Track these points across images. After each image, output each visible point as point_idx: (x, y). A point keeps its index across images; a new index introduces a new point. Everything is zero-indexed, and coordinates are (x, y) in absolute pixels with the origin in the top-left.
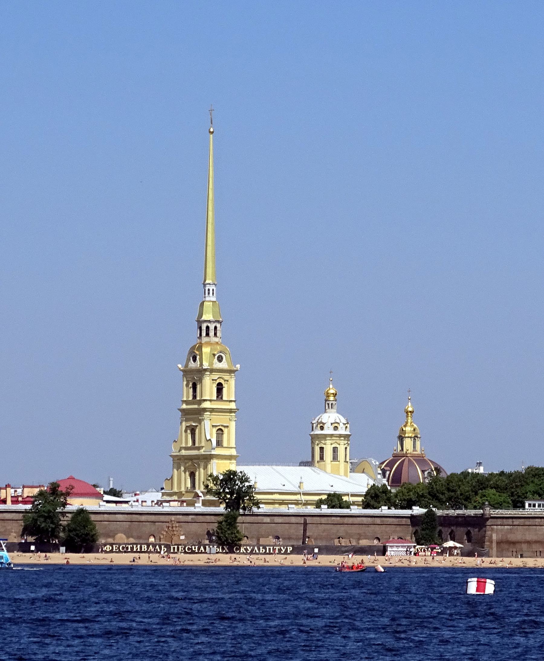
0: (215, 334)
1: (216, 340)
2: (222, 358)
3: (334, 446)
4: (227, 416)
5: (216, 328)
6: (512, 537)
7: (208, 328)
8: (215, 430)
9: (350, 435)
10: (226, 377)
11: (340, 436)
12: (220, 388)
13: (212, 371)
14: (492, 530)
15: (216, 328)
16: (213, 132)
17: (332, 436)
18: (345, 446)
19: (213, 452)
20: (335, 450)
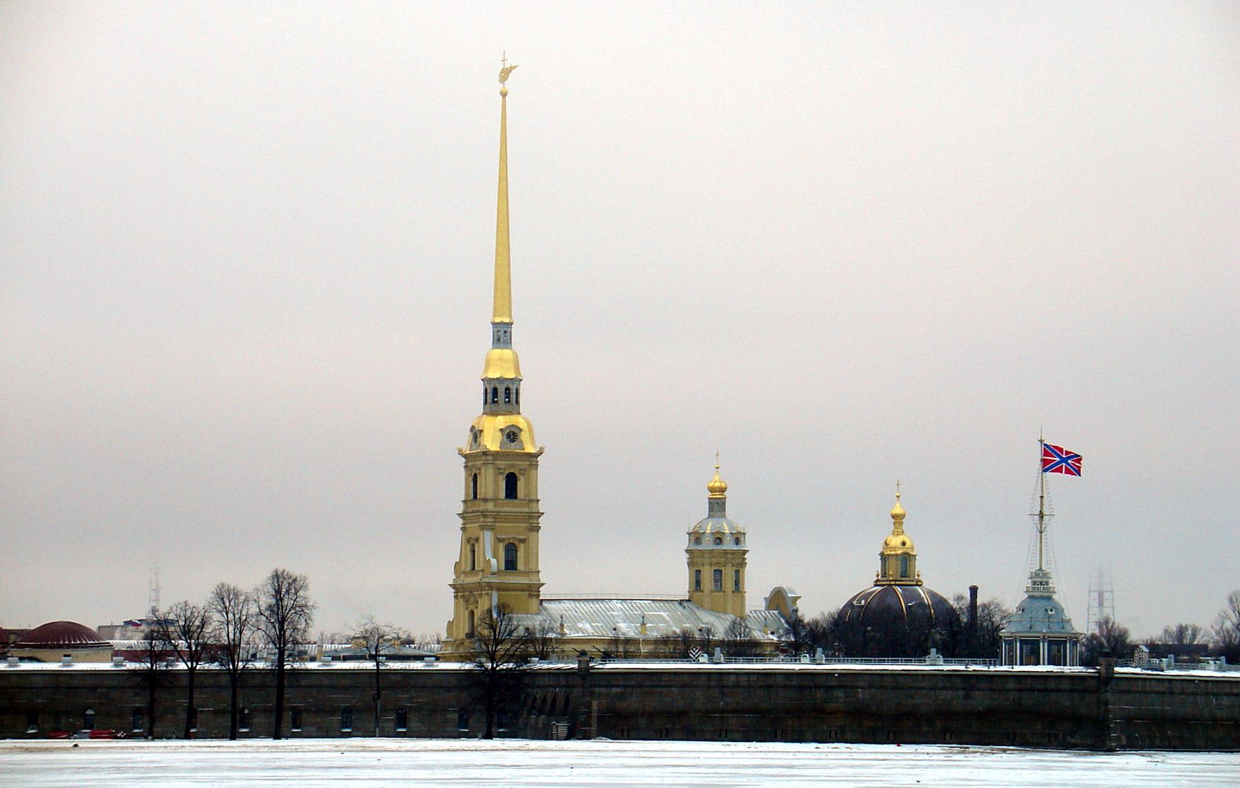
1: (509, 407)
5: (507, 389)
6: (623, 705)
7: (495, 390)
8: (501, 547)
10: (523, 464)
11: (726, 552)
13: (496, 455)
14: (592, 694)
15: (507, 389)
19: (494, 580)
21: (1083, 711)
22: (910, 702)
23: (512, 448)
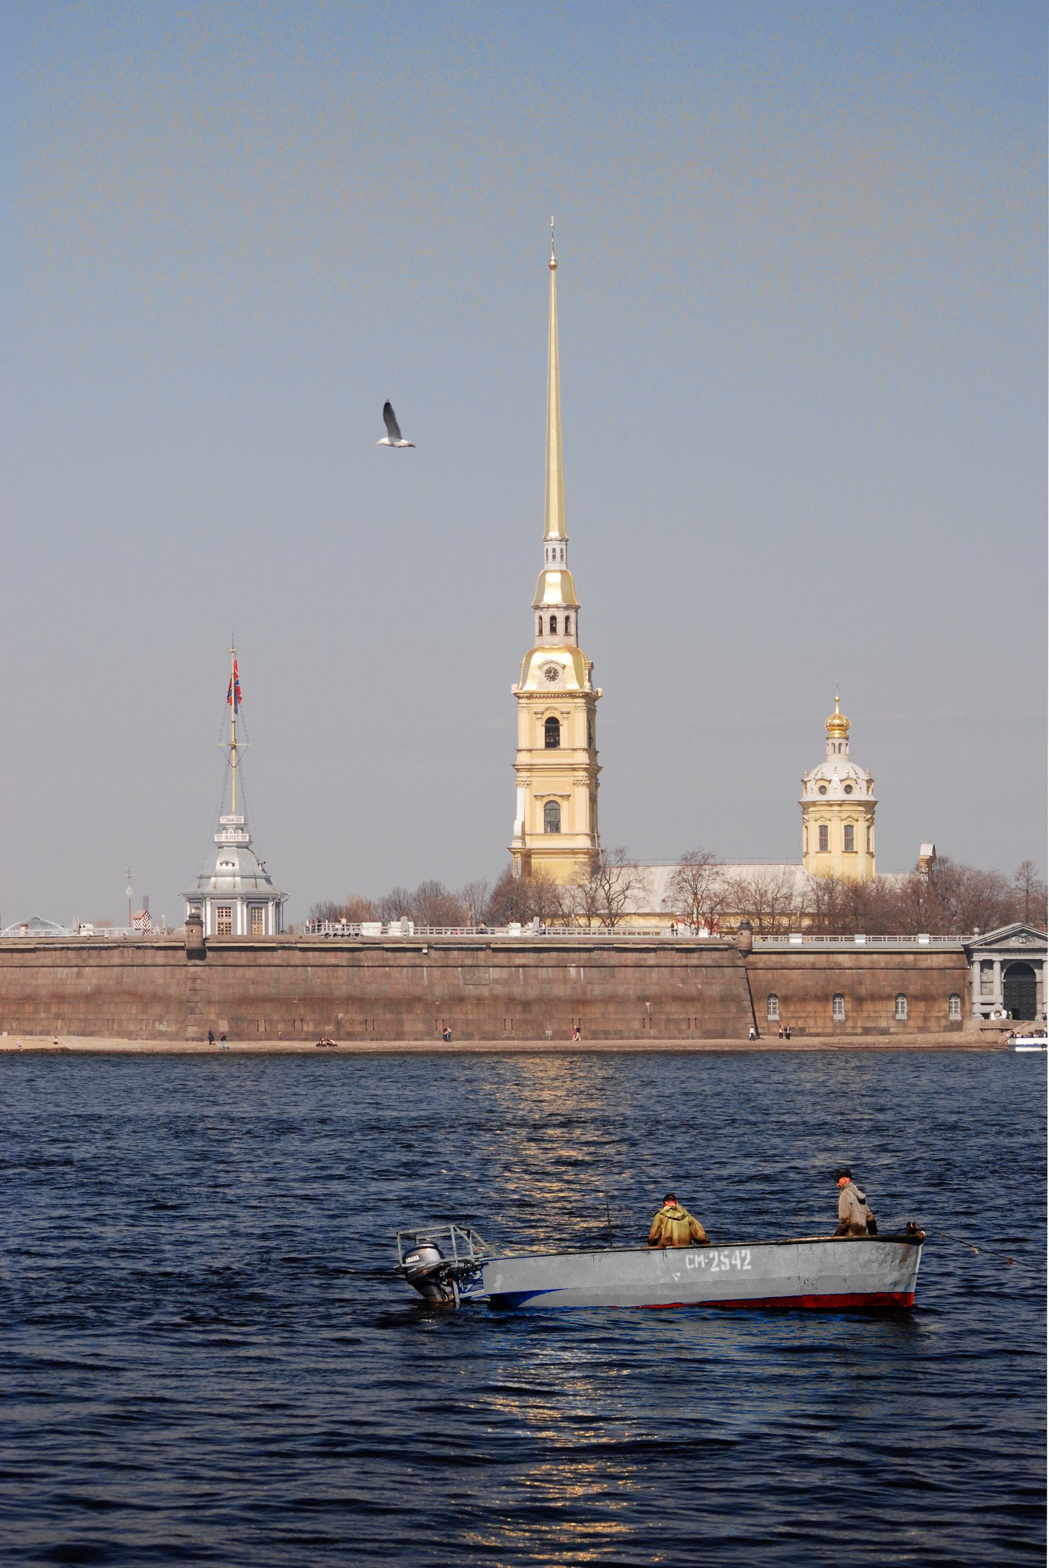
0: (553, 630)
2: (556, 672)
3: (820, 823)
4: (569, 777)
5: (553, 619)
8: (540, 806)
9: (875, 803)
10: (565, 704)
12: (552, 727)
13: (531, 696)
15: (553, 619)
16: (554, 267)
17: (814, 804)
18: (845, 823)
20: (823, 829)
21: (173, 991)
22: (34, 982)
23: (553, 687)
